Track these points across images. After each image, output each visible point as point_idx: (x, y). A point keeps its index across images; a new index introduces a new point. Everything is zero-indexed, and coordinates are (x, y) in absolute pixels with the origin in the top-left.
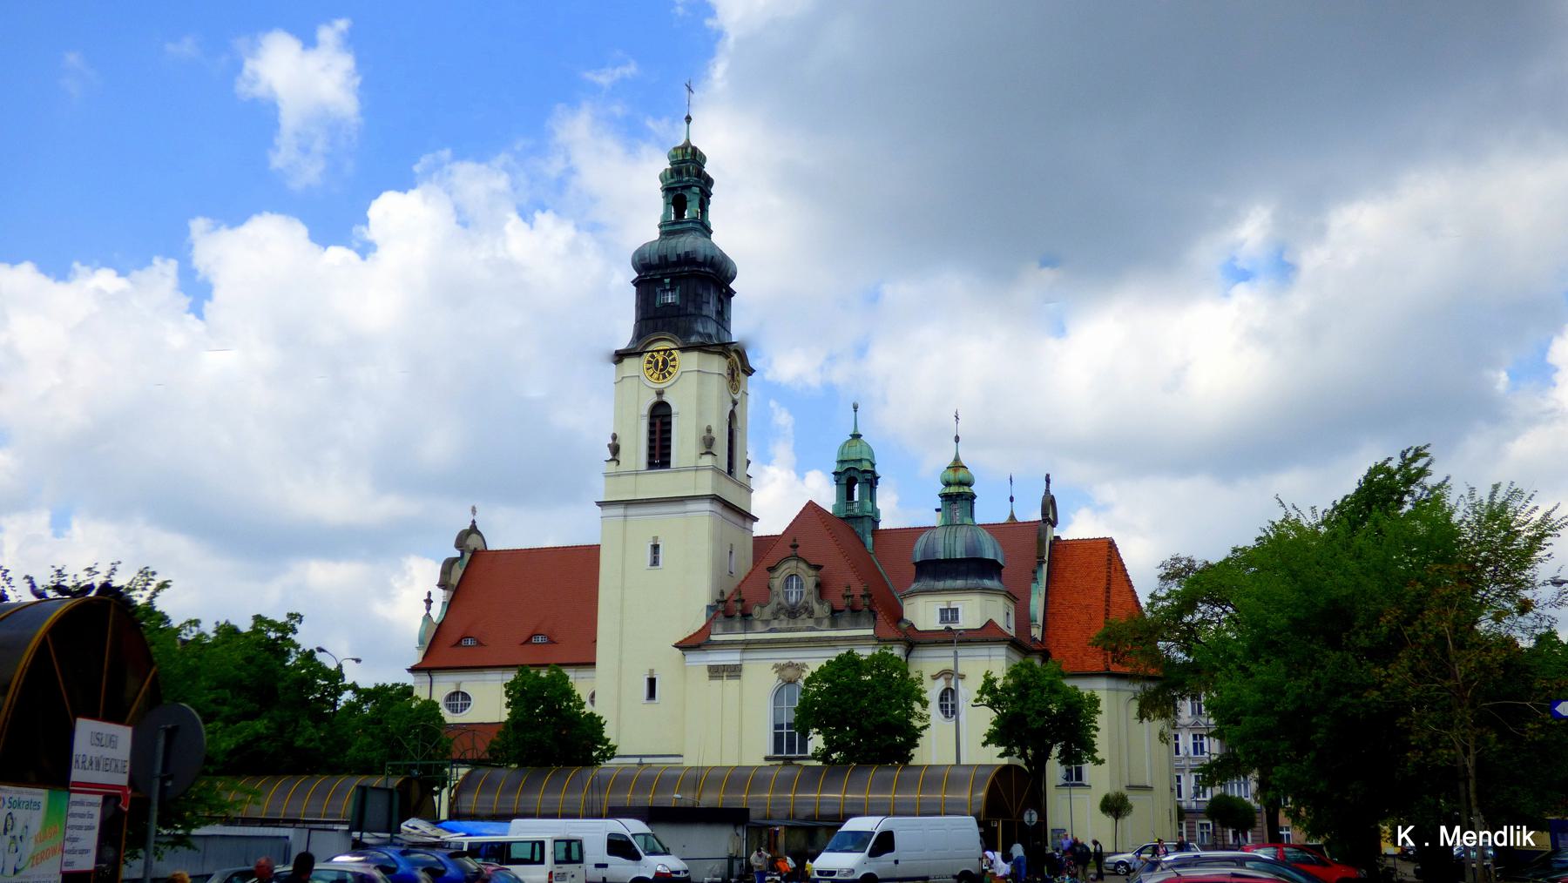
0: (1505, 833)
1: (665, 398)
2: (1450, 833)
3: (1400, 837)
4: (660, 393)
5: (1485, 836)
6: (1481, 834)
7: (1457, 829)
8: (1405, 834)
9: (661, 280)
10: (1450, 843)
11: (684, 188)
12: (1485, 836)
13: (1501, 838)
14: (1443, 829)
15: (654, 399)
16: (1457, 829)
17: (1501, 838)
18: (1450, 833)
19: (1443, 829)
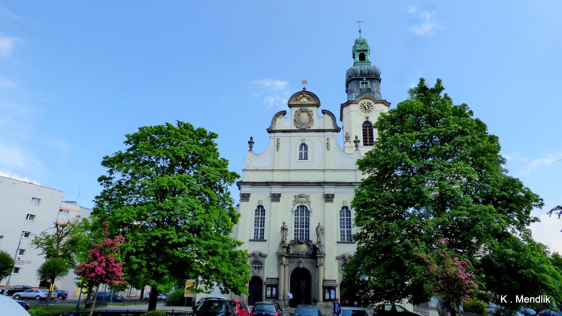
0: (539, 298)
1: (369, 120)
2: (520, 298)
3: (502, 299)
4: (367, 118)
5: (532, 299)
6: (531, 298)
7: (522, 297)
8: (504, 299)
9: (362, 79)
10: (520, 302)
11: (364, 51)
12: (532, 299)
13: (538, 300)
14: (517, 297)
15: (365, 120)
16: (522, 297)
17: (538, 300)
18: (520, 298)
19: (517, 297)
